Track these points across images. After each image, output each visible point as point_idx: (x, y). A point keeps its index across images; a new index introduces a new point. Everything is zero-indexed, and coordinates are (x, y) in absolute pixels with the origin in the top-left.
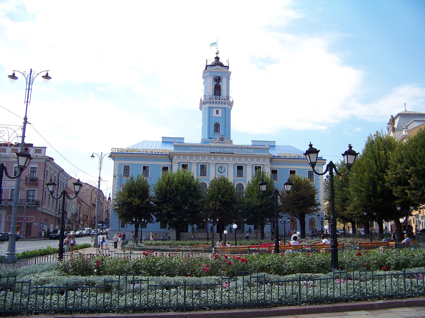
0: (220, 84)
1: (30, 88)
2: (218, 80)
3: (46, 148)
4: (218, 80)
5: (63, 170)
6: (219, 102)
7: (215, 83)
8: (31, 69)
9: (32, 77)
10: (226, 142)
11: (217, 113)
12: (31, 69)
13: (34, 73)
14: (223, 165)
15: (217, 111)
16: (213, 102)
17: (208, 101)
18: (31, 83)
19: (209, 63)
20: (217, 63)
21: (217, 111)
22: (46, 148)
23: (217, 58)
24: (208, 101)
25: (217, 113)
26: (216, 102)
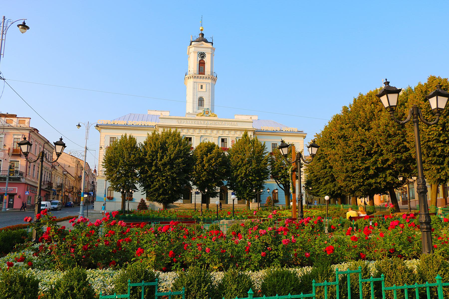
0: (204, 59)
1: (4, 38)
2: (202, 55)
3: (30, 118)
4: (202, 55)
5: (48, 141)
6: (203, 77)
7: (199, 59)
8: (4, 17)
9: (5, 26)
10: (209, 116)
11: (202, 88)
12: (4, 17)
13: (8, 22)
14: (208, 138)
15: (202, 86)
16: (198, 77)
17: (192, 76)
18: (4, 33)
19: (195, 39)
20: (202, 39)
21: (202, 86)
22: (30, 118)
23: (203, 35)
24: (192, 76)
25: (202, 88)
26: (201, 77)
